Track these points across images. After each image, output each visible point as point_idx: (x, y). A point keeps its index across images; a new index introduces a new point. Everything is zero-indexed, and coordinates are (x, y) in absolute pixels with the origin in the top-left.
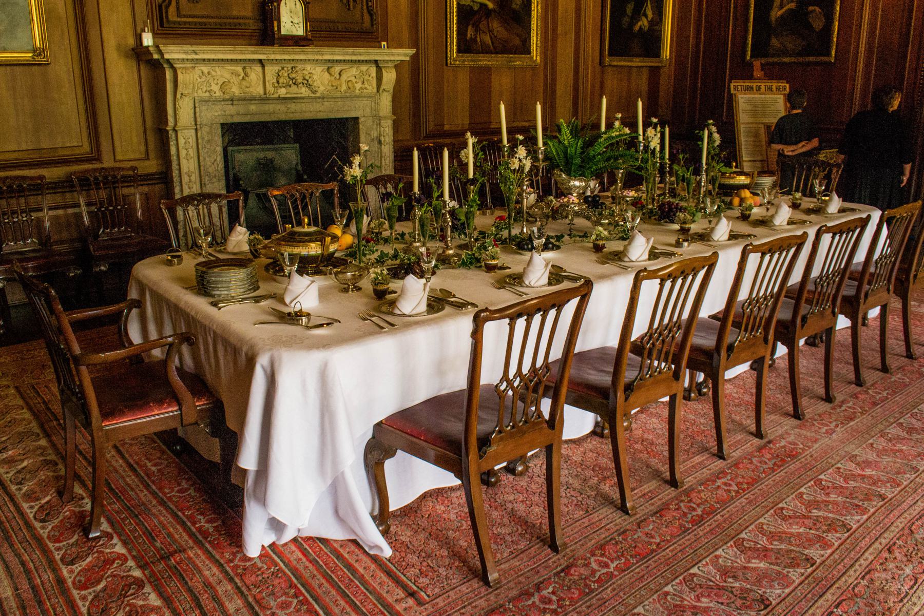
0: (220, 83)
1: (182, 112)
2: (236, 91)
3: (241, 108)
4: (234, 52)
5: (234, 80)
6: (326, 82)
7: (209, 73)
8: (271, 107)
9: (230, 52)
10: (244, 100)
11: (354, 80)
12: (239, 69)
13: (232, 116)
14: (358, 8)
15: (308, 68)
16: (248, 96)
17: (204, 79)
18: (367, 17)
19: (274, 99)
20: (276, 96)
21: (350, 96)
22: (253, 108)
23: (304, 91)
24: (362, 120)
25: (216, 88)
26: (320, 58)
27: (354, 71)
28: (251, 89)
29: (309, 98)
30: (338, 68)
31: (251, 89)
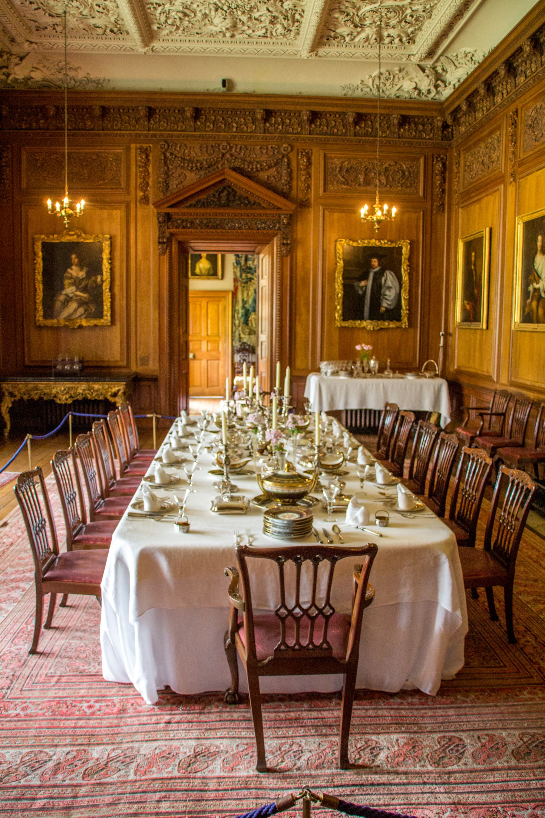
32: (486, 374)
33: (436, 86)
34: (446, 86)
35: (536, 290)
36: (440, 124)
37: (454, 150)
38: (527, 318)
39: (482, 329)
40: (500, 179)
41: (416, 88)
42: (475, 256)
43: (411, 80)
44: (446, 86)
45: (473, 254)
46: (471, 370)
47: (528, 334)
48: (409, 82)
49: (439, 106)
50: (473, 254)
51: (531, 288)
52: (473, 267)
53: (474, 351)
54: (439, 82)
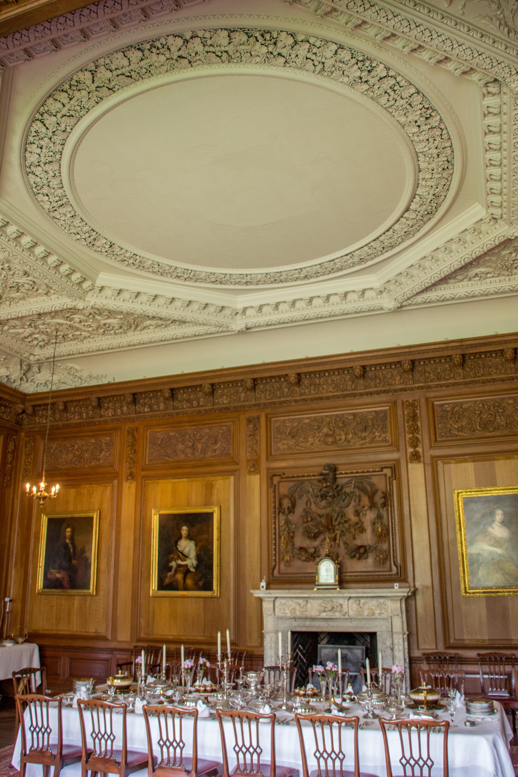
0: (291, 608)
1: (269, 623)
2: (298, 614)
3: (301, 623)
4: (289, 593)
5: (298, 608)
6: (355, 609)
7: (285, 604)
8: (317, 623)
9: (286, 593)
10: (301, 618)
11: (374, 608)
12: (301, 601)
13: (295, 627)
14: (388, 562)
15: (341, 601)
16: (304, 616)
17: (281, 607)
18: (394, 568)
19: (319, 619)
20: (320, 617)
21: (371, 618)
22: (308, 623)
23: (338, 615)
24: (378, 634)
25: (288, 611)
26: (342, 595)
27: (374, 602)
28: (307, 613)
29: (341, 618)
30: (362, 601)
31: (307, 613)
32: (95, 634)
33: (21, 379)
34: (27, 381)
35: (179, 566)
36: (20, 411)
37: (23, 434)
38: (162, 586)
39: (92, 596)
40: (116, 476)
41: (7, 376)
42: (73, 532)
43: (8, 368)
44: (27, 381)
45: (69, 530)
46: (62, 633)
47: (193, 599)
48: (6, 369)
49: (23, 397)
50: (69, 530)
51: (173, 564)
52: (68, 541)
53: (69, 615)
54: (24, 377)
